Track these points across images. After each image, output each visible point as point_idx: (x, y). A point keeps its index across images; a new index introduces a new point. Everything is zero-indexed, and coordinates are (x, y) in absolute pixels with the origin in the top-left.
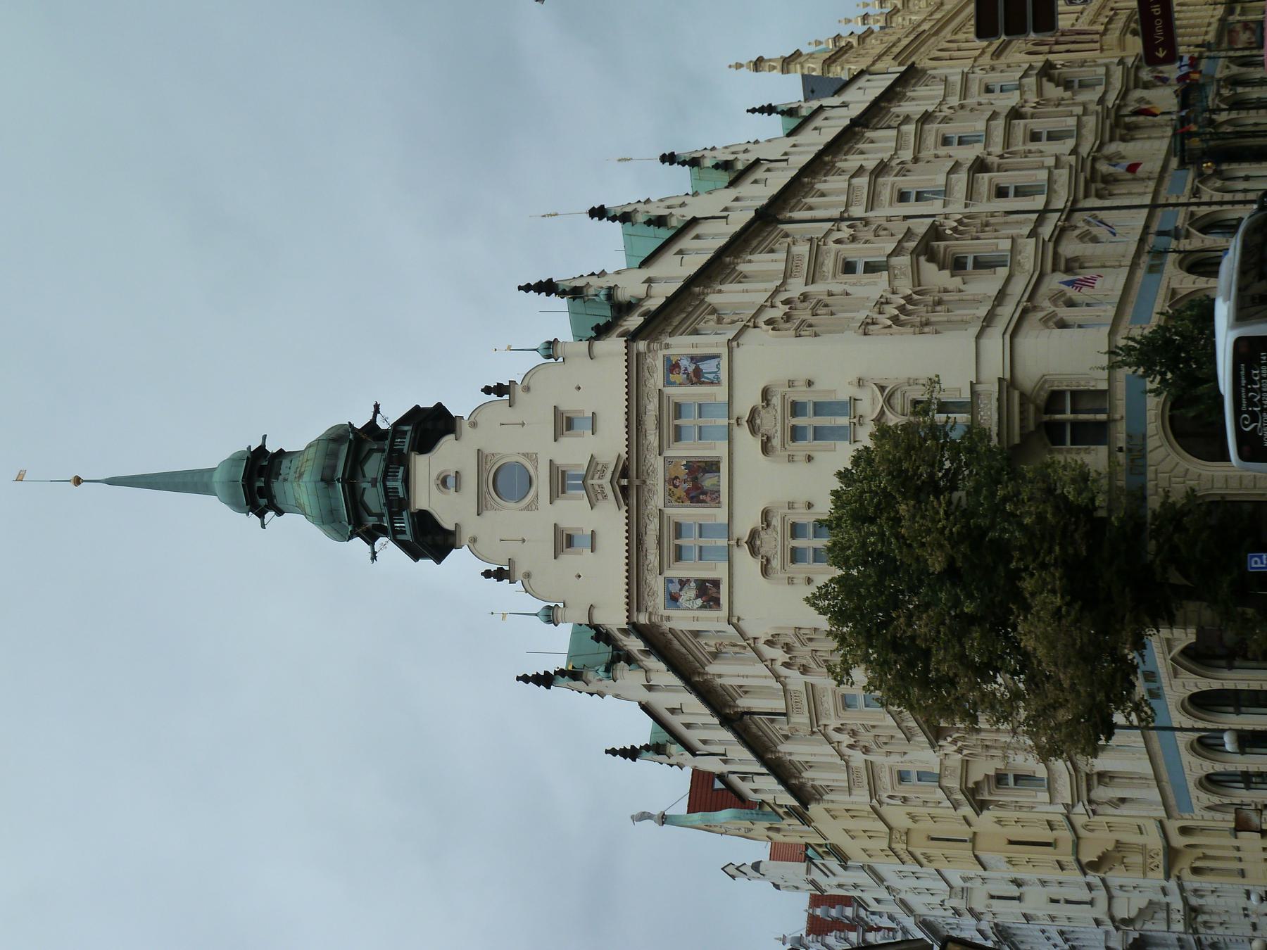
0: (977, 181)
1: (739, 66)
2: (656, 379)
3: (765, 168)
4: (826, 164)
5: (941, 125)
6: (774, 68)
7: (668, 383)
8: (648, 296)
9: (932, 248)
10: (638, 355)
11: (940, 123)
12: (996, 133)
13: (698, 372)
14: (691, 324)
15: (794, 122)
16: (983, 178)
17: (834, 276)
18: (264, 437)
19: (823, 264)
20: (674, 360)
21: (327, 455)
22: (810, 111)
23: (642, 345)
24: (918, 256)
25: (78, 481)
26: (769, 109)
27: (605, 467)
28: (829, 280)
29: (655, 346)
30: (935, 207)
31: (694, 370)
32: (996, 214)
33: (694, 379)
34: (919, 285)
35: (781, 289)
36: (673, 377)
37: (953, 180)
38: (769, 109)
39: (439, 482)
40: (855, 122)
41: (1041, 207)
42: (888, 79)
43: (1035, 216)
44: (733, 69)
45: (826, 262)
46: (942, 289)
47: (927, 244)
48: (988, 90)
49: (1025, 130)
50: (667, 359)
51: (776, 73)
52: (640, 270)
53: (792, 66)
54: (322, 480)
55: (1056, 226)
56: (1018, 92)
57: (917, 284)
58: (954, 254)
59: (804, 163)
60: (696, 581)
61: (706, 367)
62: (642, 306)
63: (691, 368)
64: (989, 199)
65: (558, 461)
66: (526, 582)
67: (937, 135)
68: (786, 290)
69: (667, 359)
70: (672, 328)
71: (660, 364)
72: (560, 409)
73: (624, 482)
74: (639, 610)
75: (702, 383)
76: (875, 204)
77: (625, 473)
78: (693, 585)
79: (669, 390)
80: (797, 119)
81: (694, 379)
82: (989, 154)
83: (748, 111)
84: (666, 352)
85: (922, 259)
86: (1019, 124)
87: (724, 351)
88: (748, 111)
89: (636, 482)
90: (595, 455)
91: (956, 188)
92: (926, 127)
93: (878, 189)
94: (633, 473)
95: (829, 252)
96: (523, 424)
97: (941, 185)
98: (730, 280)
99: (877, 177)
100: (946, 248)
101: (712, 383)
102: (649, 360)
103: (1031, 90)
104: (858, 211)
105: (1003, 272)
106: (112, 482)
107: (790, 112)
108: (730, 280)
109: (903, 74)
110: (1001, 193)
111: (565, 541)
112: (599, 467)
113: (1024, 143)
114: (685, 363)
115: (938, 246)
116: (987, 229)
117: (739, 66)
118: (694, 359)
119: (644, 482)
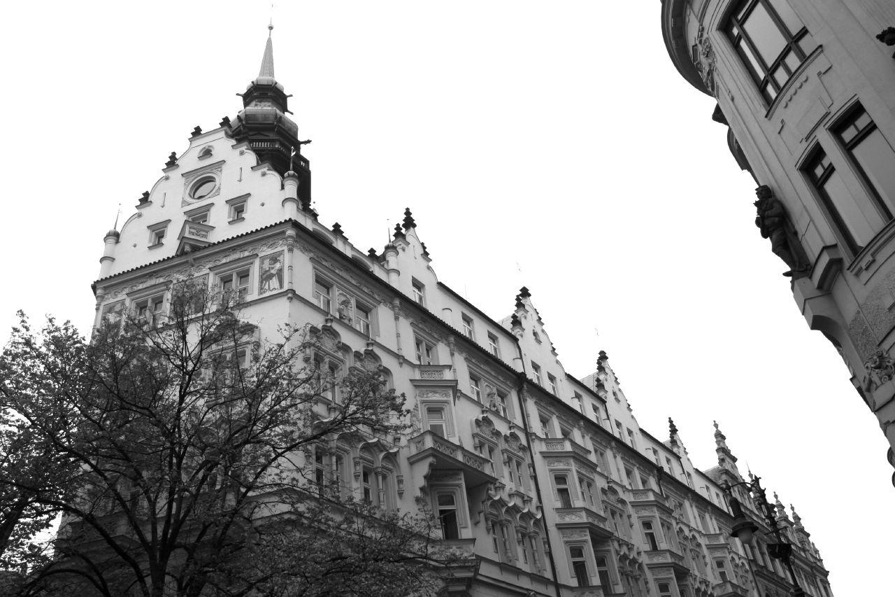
0: (581, 532)
1: (716, 425)
2: (266, 251)
3: (598, 404)
4: (610, 444)
5: (659, 520)
6: (718, 445)
7: (263, 259)
8: (388, 271)
9: (457, 474)
10: (284, 232)
11: (660, 518)
12: (660, 558)
13: (270, 277)
14: (337, 282)
15: (669, 445)
16: (585, 535)
17: (423, 402)
18: (291, 96)
19: (435, 392)
20: (281, 258)
21: (265, 115)
22: (677, 452)
23: (291, 232)
24: (433, 455)
25: (271, 28)
26: (674, 430)
27: (203, 236)
28: (418, 399)
29: (290, 241)
30: (552, 501)
31: (272, 274)
32: (547, 546)
33: (265, 275)
34: (412, 464)
35: (401, 361)
36: (267, 262)
37: (581, 513)
38: (674, 430)
39: (207, 148)
40: (660, 470)
41: (561, 581)
42: (720, 502)
43: (548, 575)
44: (713, 423)
45: (437, 395)
46: (400, 478)
47: (461, 470)
48: (720, 564)
49: (668, 578)
50: (281, 253)
51: (716, 446)
52: (435, 283)
53: (721, 454)
54: (246, 115)
55: (527, 590)
56: (721, 582)
57: (412, 460)
58: (454, 493)
59: (604, 428)
60: (120, 320)
61: (274, 283)
62: (336, 239)
63: (273, 272)
64: (566, 542)
65: (213, 210)
66: (136, 216)
67: (650, 517)
68: (401, 364)
69: (281, 253)
70: (331, 267)
71: (279, 249)
72: (249, 198)
73: (187, 248)
74: (105, 288)
75: (262, 282)
76: (550, 459)
77: (195, 249)
78: (118, 319)
79: (257, 262)
80: (673, 448)
81: (265, 275)
82: (639, 553)
83: (670, 418)
84: (286, 251)
85: (431, 460)
86: (671, 574)
87: (286, 287)
88: (670, 418)
89: (190, 258)
90: (215, 229)
91: (574, 517)
92: (655, 509)
93: (563, 460)
94: (198, 255)
95: (446, 396)
96: (240, 181)
97: (574, 504)
98: (416, 330)
99: (574, 457)
100: (459, 486)
101: (262, 289)
102: (281, 242)
103: (724, 591)
104: (538, 447)
105: (438, 533)
106: (269, 41)
107: (673, 442)
108: (416, 330)
109: (729, 515)
110: (576, 551)
111: (159, 232)
112: (204, 233)
113: (656, 580)
114: (278, 266)
115: (461, 479)
116: (520, 535)
117: (716, 425)
118: (280, 271)
119: (193, 266)
